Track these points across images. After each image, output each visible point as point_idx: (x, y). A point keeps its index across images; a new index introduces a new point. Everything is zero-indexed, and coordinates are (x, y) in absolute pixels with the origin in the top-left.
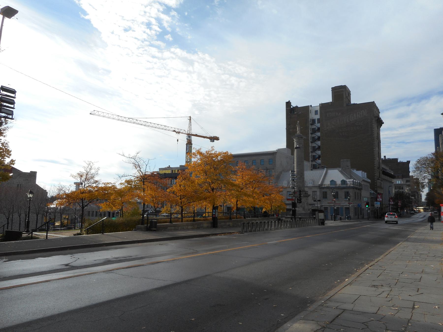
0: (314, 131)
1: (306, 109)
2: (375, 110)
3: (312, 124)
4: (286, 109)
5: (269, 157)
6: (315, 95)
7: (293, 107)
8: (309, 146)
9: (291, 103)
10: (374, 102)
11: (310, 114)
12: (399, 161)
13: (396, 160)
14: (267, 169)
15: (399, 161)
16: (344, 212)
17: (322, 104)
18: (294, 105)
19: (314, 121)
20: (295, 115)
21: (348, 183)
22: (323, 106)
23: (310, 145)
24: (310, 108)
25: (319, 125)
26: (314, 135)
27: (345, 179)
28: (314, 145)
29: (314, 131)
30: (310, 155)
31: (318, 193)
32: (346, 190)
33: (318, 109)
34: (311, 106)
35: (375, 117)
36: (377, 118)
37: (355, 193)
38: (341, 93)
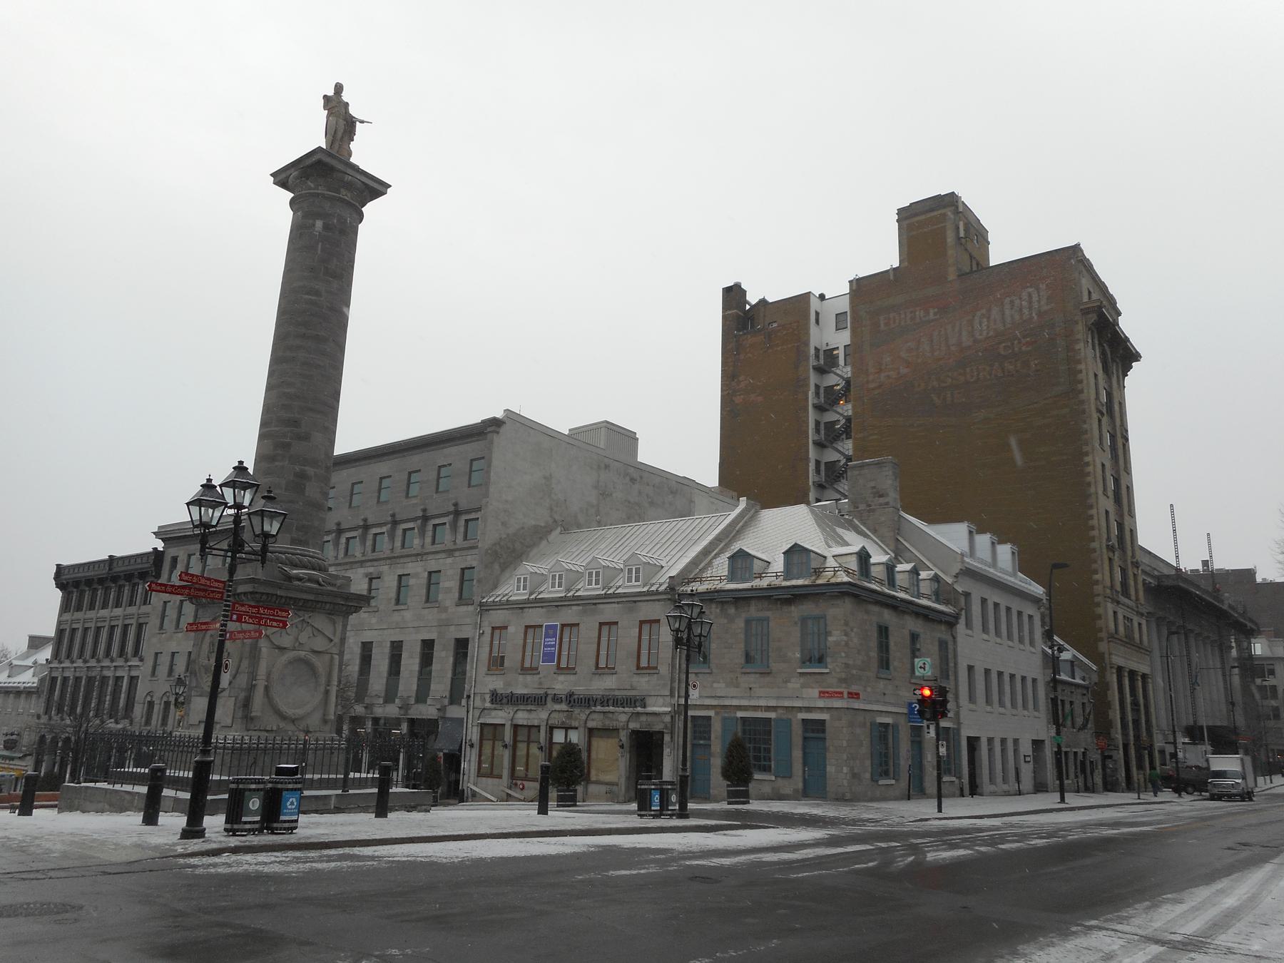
0: (831, 398)
1: (798, 306)
2: (1085, 283)
3: (821, 371)
4: (724, 317)
5: (471, 449)
6: (832, 250)
7: (753, 307)
8: (807, 459)
9: (744, 292)
10: (1076, 249)
11: (813, 329)
12: (1259, 580)
13: (1249, 574)
14: (457, 513)
15: (1259, 580)
16: (797, 754)
18: (752, 298)
19: (830, 355)
20: (757, 334)
21: (831, 563)
22: (862, 288)
23: (812, 453)
24: (815, 304)
25: (847, 372)
26: (830, 417)
27: (813, 539)
28: (831, 456)
29: (831, 398)
30: (812, 496)
32: (808, 608)
33: (845, 306)
34: (822, 297)
35: (1085, 312)
36: (1093, 317)
37: (883, 631)
38: (938, 229)
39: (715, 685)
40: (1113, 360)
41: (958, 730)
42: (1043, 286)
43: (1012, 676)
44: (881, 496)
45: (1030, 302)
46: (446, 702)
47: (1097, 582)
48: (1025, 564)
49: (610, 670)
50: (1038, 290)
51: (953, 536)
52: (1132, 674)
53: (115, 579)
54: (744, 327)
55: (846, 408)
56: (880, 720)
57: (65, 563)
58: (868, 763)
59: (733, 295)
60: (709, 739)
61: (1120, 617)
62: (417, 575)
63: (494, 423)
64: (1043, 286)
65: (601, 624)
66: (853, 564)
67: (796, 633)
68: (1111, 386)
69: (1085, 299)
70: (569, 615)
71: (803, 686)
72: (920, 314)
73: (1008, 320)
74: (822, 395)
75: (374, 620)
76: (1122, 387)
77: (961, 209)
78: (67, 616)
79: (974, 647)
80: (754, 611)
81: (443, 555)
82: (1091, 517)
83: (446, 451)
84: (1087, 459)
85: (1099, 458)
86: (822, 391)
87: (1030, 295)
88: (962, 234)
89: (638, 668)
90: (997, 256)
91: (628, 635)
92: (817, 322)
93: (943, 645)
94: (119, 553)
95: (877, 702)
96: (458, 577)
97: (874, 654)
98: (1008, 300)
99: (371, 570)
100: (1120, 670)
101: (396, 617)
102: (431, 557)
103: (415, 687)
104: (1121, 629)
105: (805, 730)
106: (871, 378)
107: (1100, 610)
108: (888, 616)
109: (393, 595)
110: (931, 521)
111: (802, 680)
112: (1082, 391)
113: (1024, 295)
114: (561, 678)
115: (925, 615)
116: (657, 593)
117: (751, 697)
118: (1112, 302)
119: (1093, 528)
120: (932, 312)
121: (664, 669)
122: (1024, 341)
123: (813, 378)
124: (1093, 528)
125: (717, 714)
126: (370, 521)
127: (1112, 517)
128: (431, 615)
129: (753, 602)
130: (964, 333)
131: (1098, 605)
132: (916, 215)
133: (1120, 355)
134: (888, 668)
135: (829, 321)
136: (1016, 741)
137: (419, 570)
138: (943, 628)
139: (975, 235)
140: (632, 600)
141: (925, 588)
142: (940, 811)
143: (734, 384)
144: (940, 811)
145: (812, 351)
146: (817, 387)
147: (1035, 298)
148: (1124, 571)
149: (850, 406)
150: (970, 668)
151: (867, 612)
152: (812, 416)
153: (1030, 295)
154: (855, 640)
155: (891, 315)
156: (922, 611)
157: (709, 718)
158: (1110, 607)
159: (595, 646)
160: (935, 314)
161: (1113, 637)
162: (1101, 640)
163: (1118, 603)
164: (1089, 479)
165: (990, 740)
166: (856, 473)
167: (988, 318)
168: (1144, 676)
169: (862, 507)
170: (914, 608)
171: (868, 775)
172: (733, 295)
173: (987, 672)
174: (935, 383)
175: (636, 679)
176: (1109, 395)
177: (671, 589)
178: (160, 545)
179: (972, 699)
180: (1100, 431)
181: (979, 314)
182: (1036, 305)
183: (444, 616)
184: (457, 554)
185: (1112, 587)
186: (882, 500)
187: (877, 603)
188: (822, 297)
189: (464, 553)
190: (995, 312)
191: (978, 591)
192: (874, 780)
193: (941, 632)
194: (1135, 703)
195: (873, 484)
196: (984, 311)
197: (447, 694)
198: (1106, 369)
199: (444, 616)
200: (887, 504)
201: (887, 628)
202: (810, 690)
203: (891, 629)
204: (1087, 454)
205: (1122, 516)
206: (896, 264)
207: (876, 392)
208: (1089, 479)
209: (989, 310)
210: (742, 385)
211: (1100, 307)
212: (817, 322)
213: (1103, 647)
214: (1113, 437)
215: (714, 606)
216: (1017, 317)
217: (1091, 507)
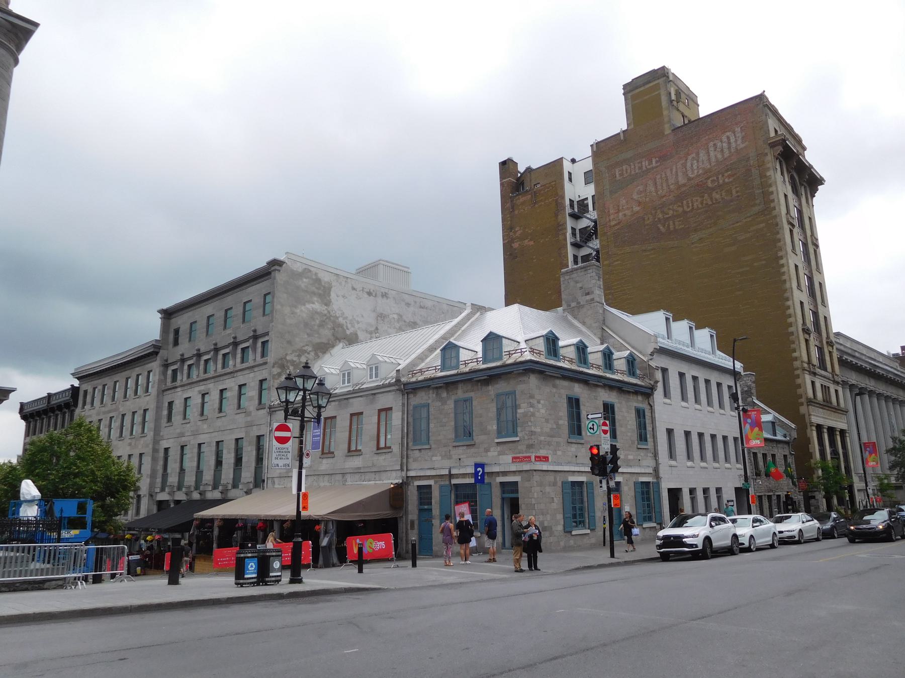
2: (772, 124)
3: (576, 217)
4: (502, 185)
7: (522, 174)
14: (255, 337)
17: (598, 144)
19: (583, 204)
20: (525, 191)
22: (601, 150)
24: (567, 166)
31: (396, 418)
32: (501, 386)
33: (588, 165)
35: (773, 145)
36: (780, 149)
37: (574, 403)
39: (434, 458)
40: (801, 185)
41: (658, 484)
42: (738, 129)
43: (713, 437)
44: (588, 294)
45: (729, 143)
46: (251, 486)
47: (796, 359)
48: (725, 344)
49: (358, 452)
50: (734, 132)
51: (652, 323)
52: (831, 430)
53: (52, 410)
54: (518, 190)
55: (595, 244)
56: (572, 478)
57: (25, 401)
58: (560, 517)
59: (507, 166)
60: (430, 504)
61: (818, 386)
62: (231, 389)
63: (275, 264)
64: (738, 129)
65: (352, 415)
66: (541, 345)
67: (493, 408)
68: (800, 204)
69: (772, 134)
71: (501, 453)
72: (645, 163)
73: (713, 159)
74: (578, 236)
75: (205, 426)
76: (810, 205)
77: (671, 78)
78: (28, 439)
79: (671, 412)
80: (461, 393)
82: (788, 307)
84: (782, 262)
85: (794, 260)
86: (578, 232)
87: (728, 138)
88: (673, 97)
89: (378, 448)
90: (704, 110)
91: (370, 422)
92: (570, 180)
93: (640, 414)
94: (53, 391)
95: (569, 463)
96: (257, 388)
97: (564, 422)
98: (711, 144)
100: (819, 427)
101: (219, 423)
102: (239, 373)
103: (231, 476)
104: (819, 395)
105: (503, 492)
106: (612, 217)
107: (799, 381)
108: (578, 390)
109: (217, 405)
110: (634, 312)
111: (499, 448)
112: (774, 208)
113: (724, 139)
114: (325, 461)
115: (619, 388)
116: (390, 385)
117: (461, 466)
118: (798, 140)
119: (790, 316)
120: (654, 161)
121: (396, 449)
122: (726, 174)
123: (570, 223)
124: (790, 316)
125: (436, 483)
126: (202, 350)
127: (807, 307)
128: (241, 419)
129: (460, 386)
130: (680, 174)
131: (798, 376)
132: (637, 88)
133: (807, 181)
134: (580, 433)
135: (579, 178)
136: (719, 490)
137: (232, 384)
138: (640, 398)
139: (684, 97)
140: (372, 393)
141: (620, 364)
142: (612, 556)
143: (511, 234)
144: (612, 556)
145: (567, 203)
146: (573, 229)
147: (732, 140)
148: (820, 350)
149: (598, 241)
150: (670, 432)
151: (554, 386)
152: (570, 251)
153: (728, 138)
154: (543, 411)
155: (624, 167)
156: (613, 384)
157: (430, 486)
158: (808, 378)
159: (347, 434)
160: (657, 162)
161: (810, 402)
162: (802, 404)
163: (815, 374)
164: (784, 277)
165: (692, 491)
166: (567, 277)
167: (698, 161)
168: (843, 432)
169: (573, 304)
170: (604, 381)
171: (560, 528)
172: (507, 166)
173: (687, 434)
174: (660, 216)
175: (376, 458)
176: (800, 212)
177: (398, 381)
178: (76, 383)
179: (672, 455)
180: (793, 242)
181: (690, 158)
182: (734, 145)
183: (249, 419)
184: (256, 369)
185: (809, 362)
186: (588, 297)
187: (564, 378)
188: (573, 161)
189: (261, 368)
190: (702, 154)
191: (674, 368)
192: (567, 531)
193: (638, 402)
194: (835, 453)
195: (579, 285)
196: (694, 155)
197: (252, 480)
198: (795, 190)
199: (249, 419)
200: (593, 300)
201: (577, 400)
202: (505, 457)
203: (581, 400)
204: (781, 258)
205: (816, 306)
206: (625, 128)
207: (618, 227)
208: (784, 277)
209: (698, 154)
210: (518, 234)
211: (784, 140)
212: (570, 180)
213: (803, 410)
214: (805, 245)
215: (431, 392)
216: (719, 156)
217: (787, 299)
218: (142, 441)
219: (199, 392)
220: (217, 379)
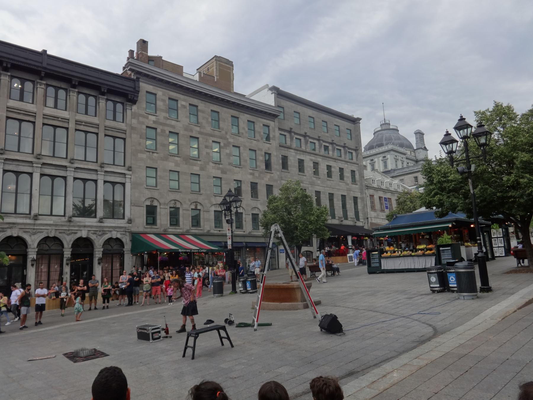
62: (334, 167)
70: (388, 195)
75: (319, 182)
81: (343, 162)
83: (343, 122)
99: (313, 158)
102: (339, 161)
103: (342, 213)
132: (222, 62)
172: (143, 44)
183: (348, 187)
184: (349, 164)
218: (268, 176)
219: (311, 160)
220: (324, 158)
